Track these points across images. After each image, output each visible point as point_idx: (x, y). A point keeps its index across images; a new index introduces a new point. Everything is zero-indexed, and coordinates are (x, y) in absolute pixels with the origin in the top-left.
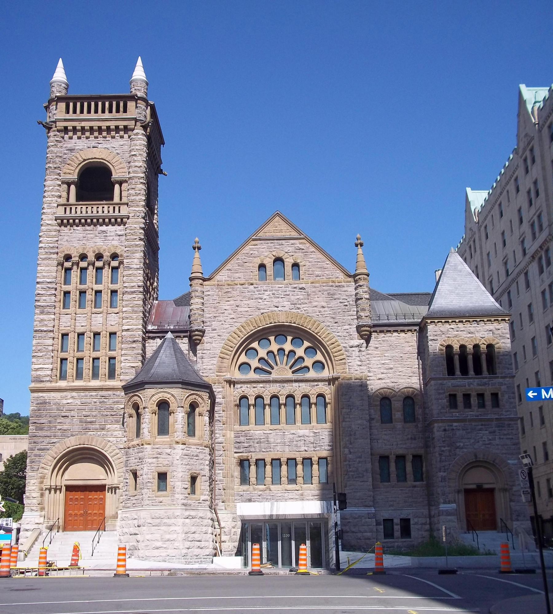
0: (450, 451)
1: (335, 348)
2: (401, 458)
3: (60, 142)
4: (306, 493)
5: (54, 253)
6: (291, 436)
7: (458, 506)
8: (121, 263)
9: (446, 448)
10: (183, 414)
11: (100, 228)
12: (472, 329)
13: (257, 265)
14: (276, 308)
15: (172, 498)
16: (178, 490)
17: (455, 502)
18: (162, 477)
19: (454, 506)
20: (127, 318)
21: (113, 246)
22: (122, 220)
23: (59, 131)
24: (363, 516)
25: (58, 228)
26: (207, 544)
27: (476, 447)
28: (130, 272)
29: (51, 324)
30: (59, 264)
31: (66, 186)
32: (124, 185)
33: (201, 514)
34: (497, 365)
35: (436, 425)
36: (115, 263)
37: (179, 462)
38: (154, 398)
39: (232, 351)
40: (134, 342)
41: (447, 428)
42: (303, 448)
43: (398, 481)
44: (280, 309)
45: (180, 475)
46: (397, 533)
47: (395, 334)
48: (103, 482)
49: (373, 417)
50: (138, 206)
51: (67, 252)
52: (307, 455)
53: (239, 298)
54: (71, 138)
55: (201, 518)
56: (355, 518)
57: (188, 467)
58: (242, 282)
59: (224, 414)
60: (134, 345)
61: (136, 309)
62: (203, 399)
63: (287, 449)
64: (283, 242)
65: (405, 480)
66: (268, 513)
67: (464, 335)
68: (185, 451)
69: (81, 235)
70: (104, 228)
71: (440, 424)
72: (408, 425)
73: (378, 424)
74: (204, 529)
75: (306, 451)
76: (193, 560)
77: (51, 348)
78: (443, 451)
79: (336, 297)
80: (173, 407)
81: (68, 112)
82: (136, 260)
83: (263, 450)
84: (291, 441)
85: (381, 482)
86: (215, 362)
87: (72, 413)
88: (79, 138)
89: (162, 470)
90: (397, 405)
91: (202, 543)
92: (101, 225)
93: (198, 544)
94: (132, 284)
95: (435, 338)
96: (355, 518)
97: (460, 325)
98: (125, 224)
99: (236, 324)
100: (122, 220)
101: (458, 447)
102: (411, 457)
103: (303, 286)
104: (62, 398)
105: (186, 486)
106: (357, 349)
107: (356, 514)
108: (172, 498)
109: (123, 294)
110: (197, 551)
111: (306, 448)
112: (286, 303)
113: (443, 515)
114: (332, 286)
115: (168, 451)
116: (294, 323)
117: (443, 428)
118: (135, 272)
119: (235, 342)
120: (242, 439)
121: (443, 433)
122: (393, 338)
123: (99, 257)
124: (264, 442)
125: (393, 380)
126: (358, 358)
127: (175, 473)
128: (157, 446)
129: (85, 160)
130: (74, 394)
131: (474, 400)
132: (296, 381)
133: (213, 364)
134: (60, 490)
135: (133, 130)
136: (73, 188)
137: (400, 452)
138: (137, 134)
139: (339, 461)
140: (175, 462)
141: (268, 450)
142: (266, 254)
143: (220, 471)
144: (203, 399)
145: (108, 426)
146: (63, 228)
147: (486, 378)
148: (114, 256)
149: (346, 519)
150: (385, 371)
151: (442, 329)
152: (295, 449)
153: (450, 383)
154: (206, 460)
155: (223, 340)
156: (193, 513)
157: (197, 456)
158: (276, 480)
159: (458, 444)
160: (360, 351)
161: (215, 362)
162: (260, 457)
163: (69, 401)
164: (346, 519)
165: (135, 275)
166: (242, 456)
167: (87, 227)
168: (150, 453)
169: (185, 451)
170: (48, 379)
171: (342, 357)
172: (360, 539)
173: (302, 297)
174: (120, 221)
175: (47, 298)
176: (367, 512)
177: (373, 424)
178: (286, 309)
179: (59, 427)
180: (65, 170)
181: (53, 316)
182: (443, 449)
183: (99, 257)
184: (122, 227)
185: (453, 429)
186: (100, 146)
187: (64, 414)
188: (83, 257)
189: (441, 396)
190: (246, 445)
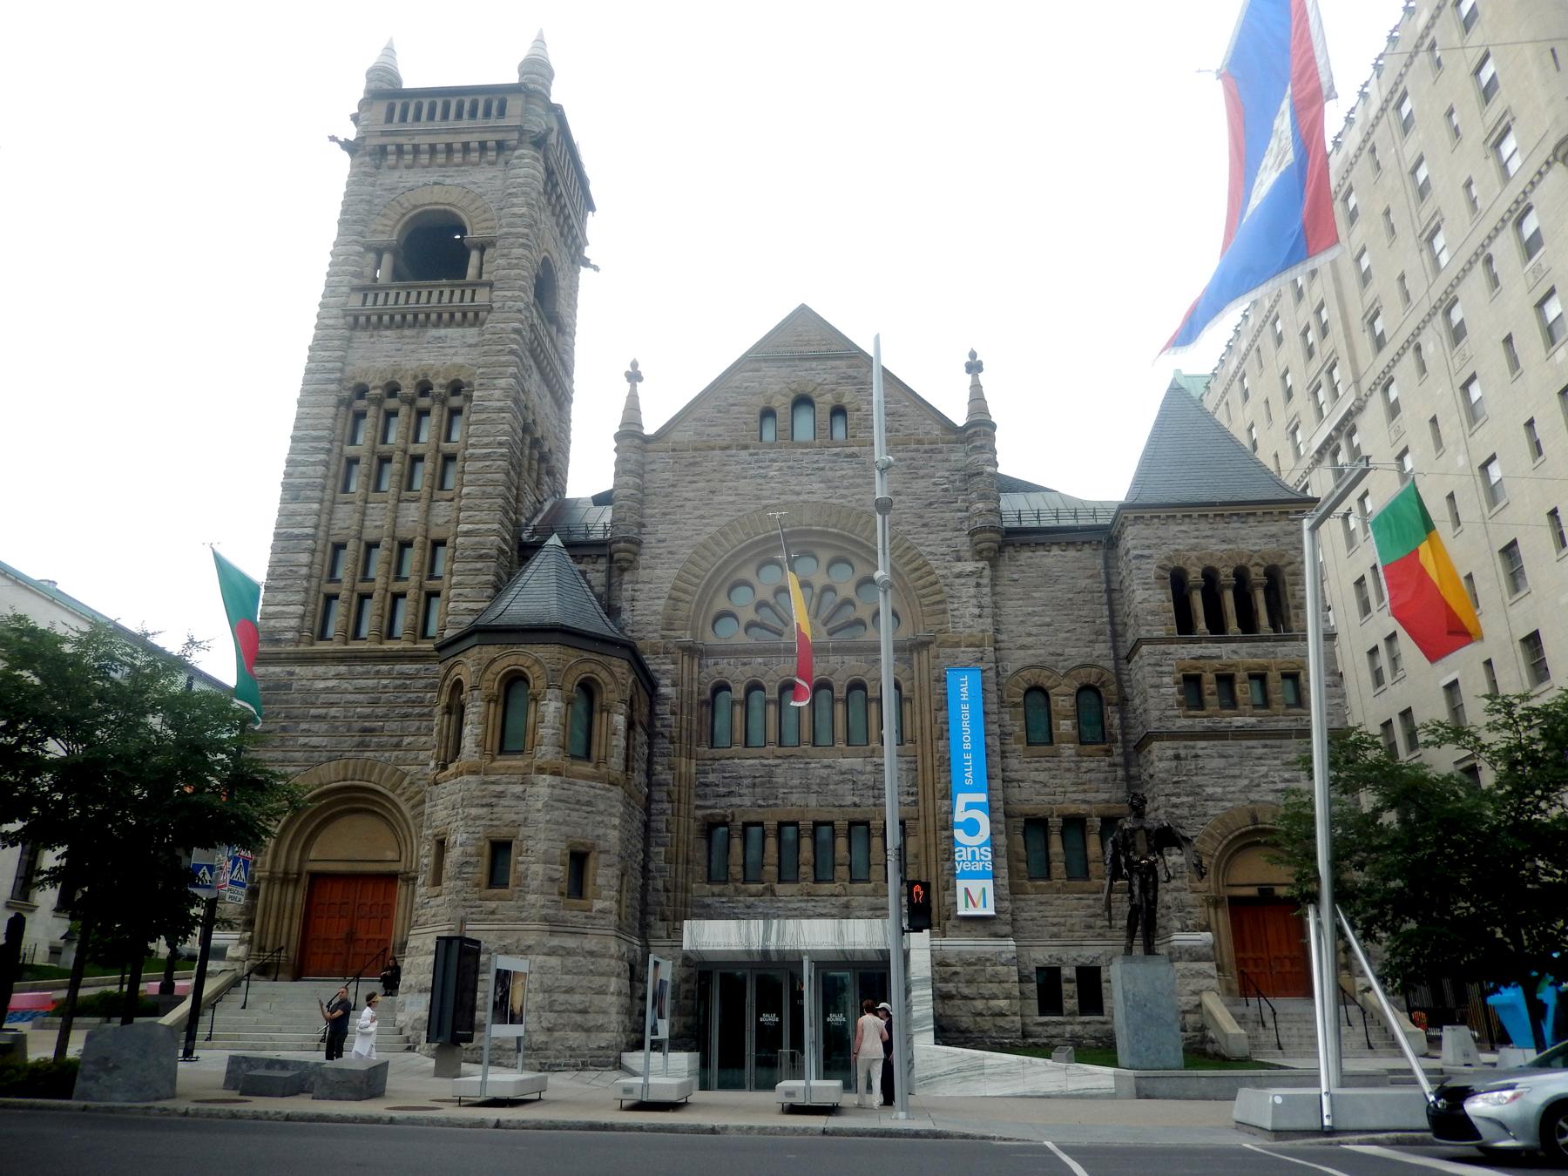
0: (1192, 806)
1: (921, 578)
2: (1074, 824)
3: (371, 175)
4: (857, 901)
5: (331, 381)
6: (824, 772)
7: (1217, 936)
8: (469, 398)
9: (1184, 799)
10: (560, 704)
11: (433, 332)
12: (1230, 534)
13: (757, 411)
14: (794, 498)
15: (521, 903)
16: (534, 884)
17: (1206, 928)
18: (500, 850)
19: (1207, 936)
20: (470, 509)
21: (454, 365)
22: (476, 315)
25: (347, 333)
26: (601, 1020)
27: (1253, 796)
28: (484, 416)
29: (312, 520)
30: (341, 402)
31: (372, 257)
32: (489, 252)
33: (591, 943)
34: (1292, 612)
35: (1155, 745)
36: (455, 401)
37: (542, 817)
38: (496, 668)
39: (697, 585)
40: (481, 557)
41: (1183, 753)
42: (849, 800)
43: (1069, 879)
44: (804, 497)
45: (542, 847)
46: (1071, 1003)
47: (1055, 551)
48: (394, 867)
49: (1008, 729)
50: (511, 289)
51: (361, 380)
52: (858, 815)
53: (719, 476)
54: (394, 168)
55: (592, 953)
56: (970, 964)
57: (564, 829)
58: (724, 444)
59: (672, 720)
60: (479, 565)
61: (489, 489)
62: (612, 674)
63: (813, 800)
64: (814, 364)
65: (1086, 875)
66: (756, 946)
67: (1215, 546)
68: (557, 792)
69: (393, 346)
70: (442, 332)
71: (1167, 744)
72: (1089, 748)
73: (1019, 746)
74: (598, 981)
75: (855, 805)
76: (562, 1061)
77: (304, 571)
78: (1175, 806)
79: (921, 472)
80: (537, 684)
81: (389, 119)
82: (497, 393)
84: (824, 782)
85: (1031, 879)
86: (660, 609)
87: (333, 711)
88: (408, 167)
89: (503, 833)
90: (1063, 701)
91: (590, 1017)
92: (436, 326)
93: (578, 1018)
94: (486, 440)
95: (1146, 552)
96: (970, 964)
97: (1204, 526)
99: (708, 529)
100: (476, 315)
102: (1097, 822)
103: (855, 449)
104: (317, 678)
105: (557, 875)
106: (972, 581)
107: (972, 953)
108: (521, 903)
109: (465, 460)
110: (575, 1038)
111: (857, 800)
112: (816, 486)
113: (1179, 959)
114: (917, 450)
115: (518, 789)
116: (834, 526)
117: (1170, 753)
118: (494, 416)
119: (705, 564)
120: (711, 778)
121: (1174, 764)
122: (1048, 561)
123: (424, 388)
124: (762, 784)
125: (1051, 650)
126: (974, 601)
127: (530, 843)
128: (493, 778)
129: (415, 207)
130: (342, 669)
131: (1245, 690)
132: (837, 650)
133: (655, 613)
134: (297, 881)
135: (515, 149)
136: (387, 259)
137: (1073, 809)
138: (520, 157)
139: (932, 828)
140: (533, 816)
142: (777, 388)
144: (612, 674)
145: (407, 740)
146: (358, 334)
147: (1268, 639)
148: (456, 388)
149: (948, 965)
150: (1034, 630)
151: (1160, 533)
152: (831, 799)
153: (1186, 652)
154: (611, 815)
155: (678, 561)
156: (570, 942)
157: (589, 803)
158: (787, 873)
159: (1209, 790)
160: (978, 585)
161: (660, 609)
163: (331, 683)
164: (948, 965)
165: (492, 422)
167: (407, 332)
168: (477, 793)
169: (557, 792)
170: (289, 635)
171: (938, 598)
172: (980, 1014)
173: (850, 472)
174: (472, 318)
175: (309, 470)
177: (1007, 748)
179: (302, 740)
180: (373, 227)
181: (316, 506)
182: (1174, 800)
183: (424, 388)
184: (474, 330)
185: (1197, 756)
186: (448, 181)
187: (313, 711)
188: (392, 390)
189: (1166, 680)
190: (722, 790)
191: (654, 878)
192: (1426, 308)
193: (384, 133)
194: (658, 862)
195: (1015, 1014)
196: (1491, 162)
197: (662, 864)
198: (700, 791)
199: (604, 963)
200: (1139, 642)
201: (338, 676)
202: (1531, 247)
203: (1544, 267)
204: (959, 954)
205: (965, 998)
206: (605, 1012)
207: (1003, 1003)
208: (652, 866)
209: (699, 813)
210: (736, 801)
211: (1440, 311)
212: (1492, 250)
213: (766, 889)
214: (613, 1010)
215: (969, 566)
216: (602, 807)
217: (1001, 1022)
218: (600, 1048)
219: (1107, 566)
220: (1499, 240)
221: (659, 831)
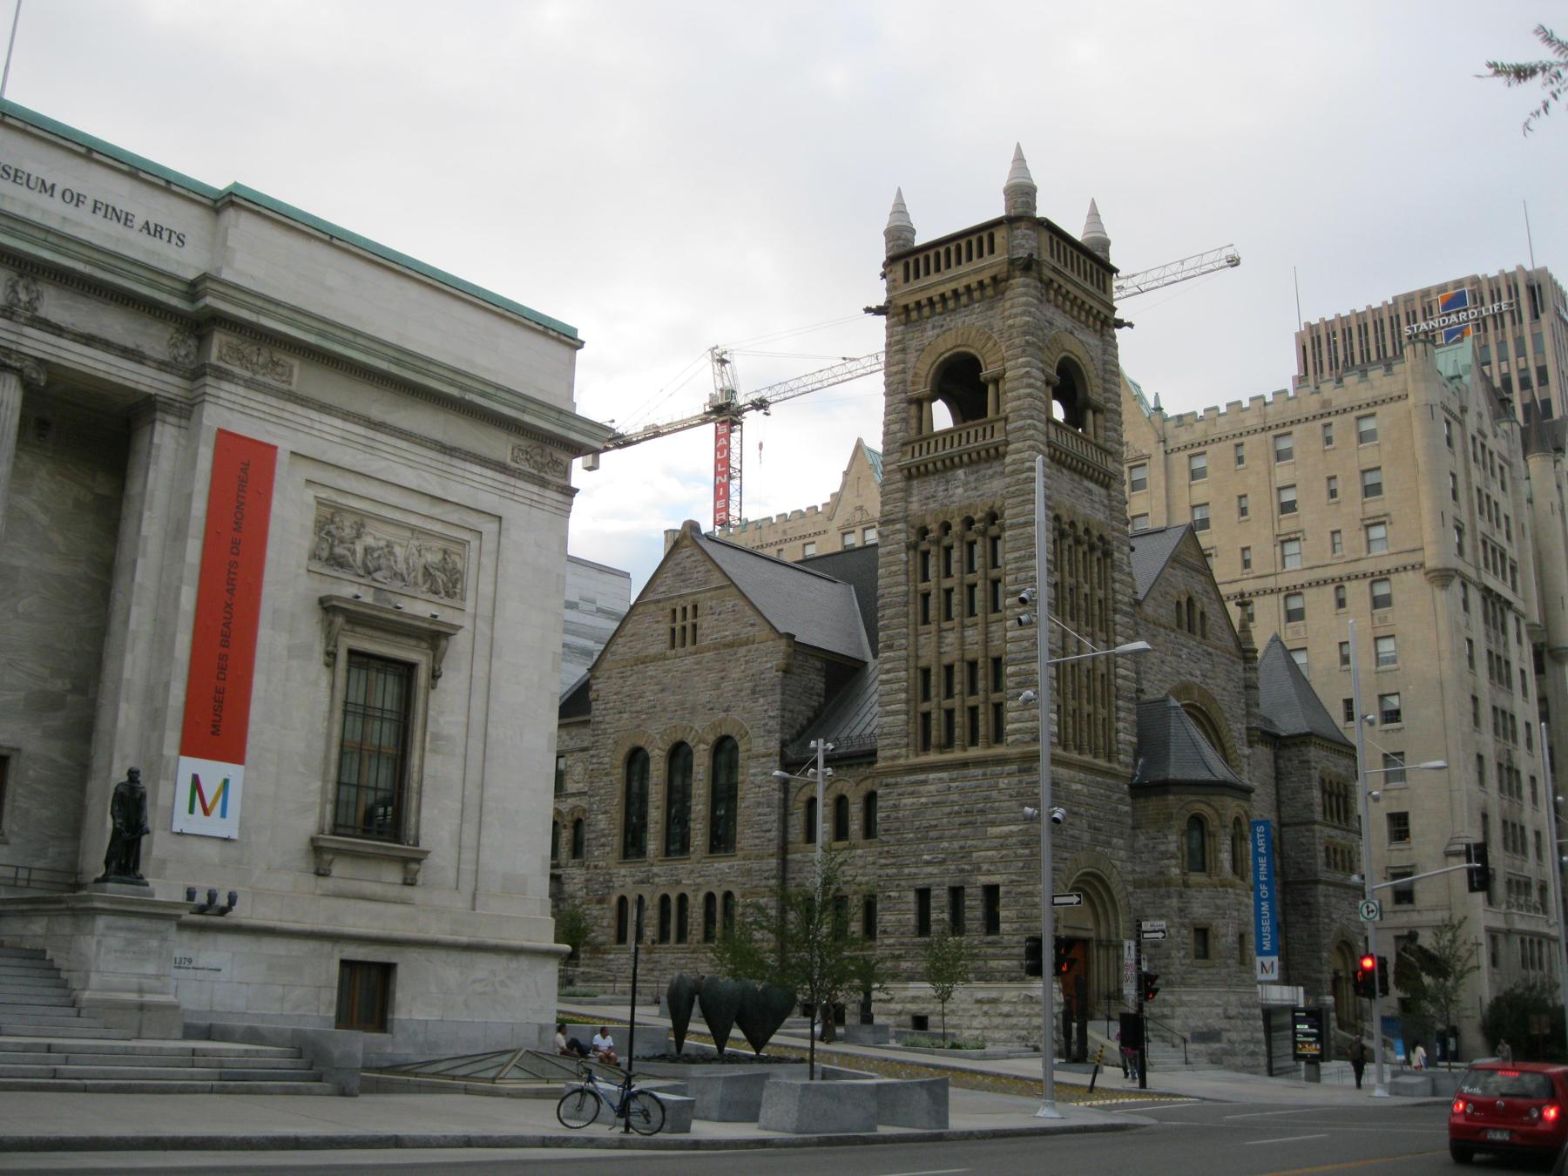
11: (1087, 483)
23: (1041, 281)
32: (1099, 416)
54: (1049, 301)
88: (1057, 306)
98: (1107, 487)
101: (1333, 920)
148: (1101, 538)
153: (1328, 831)
163: (1079, 787)
167: (1076, 477)
178: (1197, 681)
184: (1103, 491)
192: (1270, 583)
193: (1055, 270)
196: (1363, 533)
200: (1315, 822)
201: (1080, 782)
202: (1379, 602)
203: (1390, 620)
211: (1282, 595)
212: (1347, 584)
215: (1247, 751)
219: (1276, 762)
220: (1354, 583)
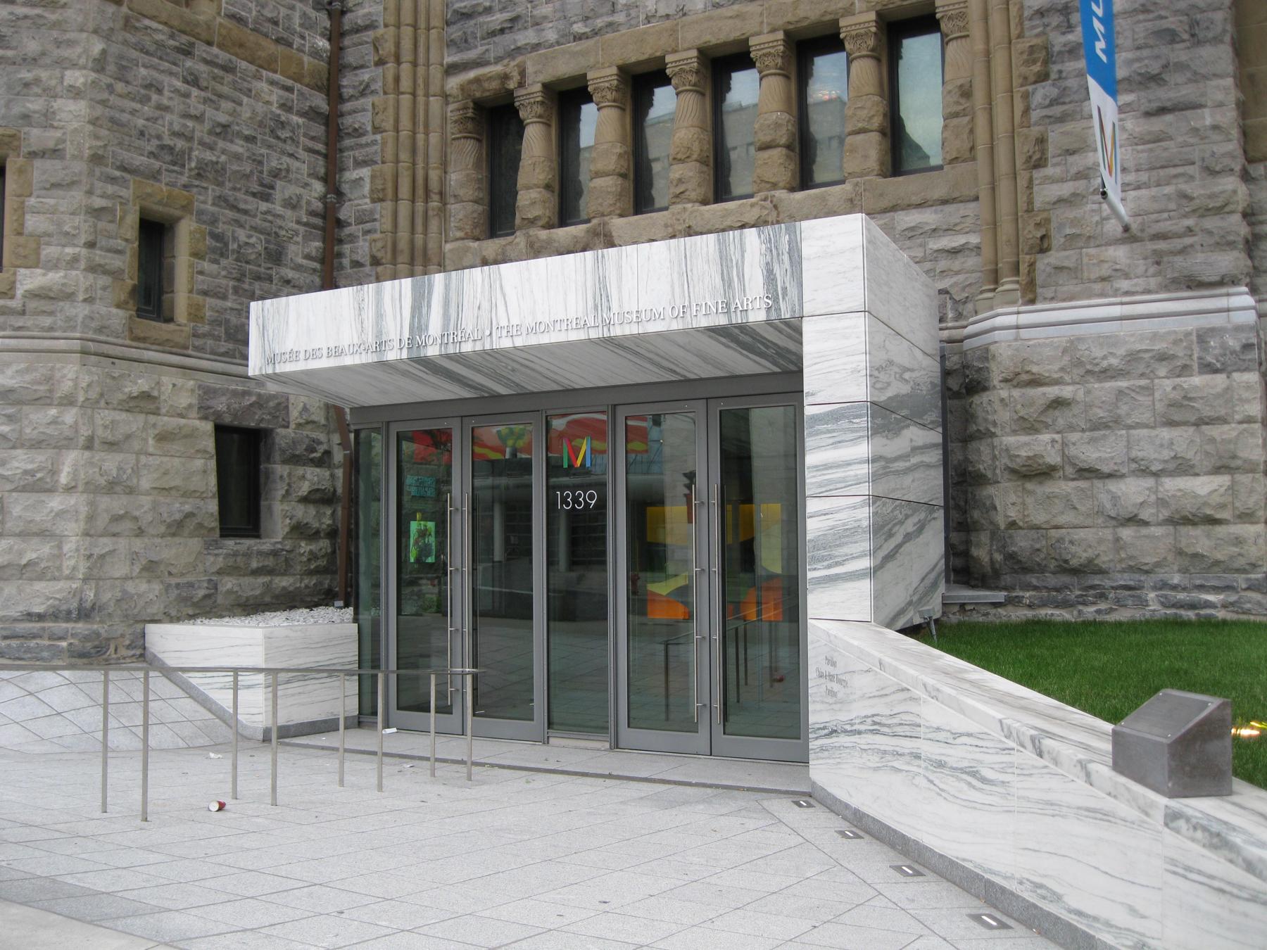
24: (1163, 357)
26: (36, 551)
56: (1107, 374)
83: (579, 28)
96: (1107, 374)
107: (1110, 341)
141: (599, 23)
143: (365, 172)
149: (1036, 382)
162: (563, 68)
164: (1036, 382)
166: (477, 80)
172: (1133, 520)
176: (1192, 324)
190: (498, 19)
191: (352, 238)
194: (358, 201)
195: (1246, 517)
197: (366, 204)
198: (455, 32)
199: (38, 419)
204: (1071, 347)
205: (1088, 473)
206: (43, 534)
207: (1205, 487)
208: (346, 212)
209: (454, 83)
210: (526, 37)
213: (595, 233)
214: (72, 530)
216: (32, 47)
217: (1199, 540)
218: (30, 616)
221: (358, 133)
